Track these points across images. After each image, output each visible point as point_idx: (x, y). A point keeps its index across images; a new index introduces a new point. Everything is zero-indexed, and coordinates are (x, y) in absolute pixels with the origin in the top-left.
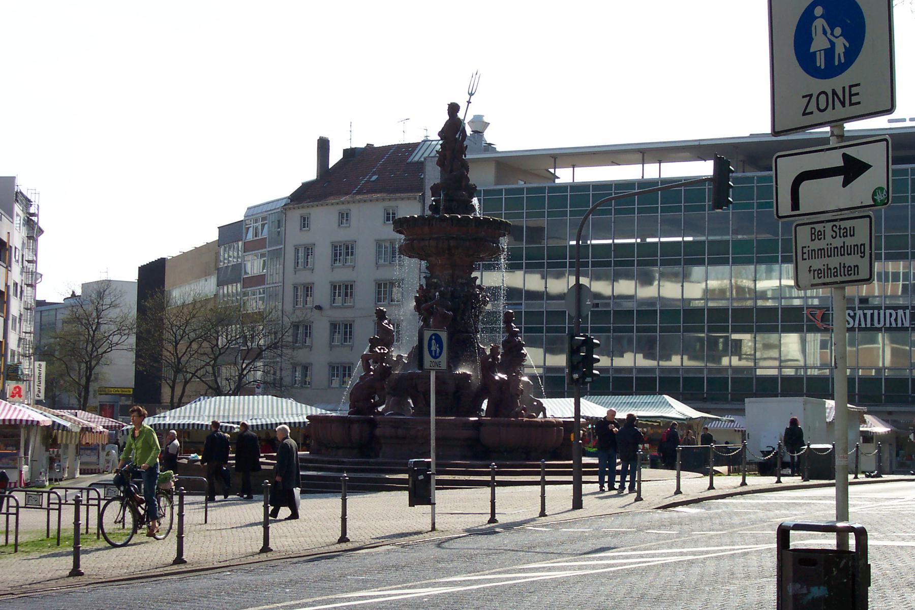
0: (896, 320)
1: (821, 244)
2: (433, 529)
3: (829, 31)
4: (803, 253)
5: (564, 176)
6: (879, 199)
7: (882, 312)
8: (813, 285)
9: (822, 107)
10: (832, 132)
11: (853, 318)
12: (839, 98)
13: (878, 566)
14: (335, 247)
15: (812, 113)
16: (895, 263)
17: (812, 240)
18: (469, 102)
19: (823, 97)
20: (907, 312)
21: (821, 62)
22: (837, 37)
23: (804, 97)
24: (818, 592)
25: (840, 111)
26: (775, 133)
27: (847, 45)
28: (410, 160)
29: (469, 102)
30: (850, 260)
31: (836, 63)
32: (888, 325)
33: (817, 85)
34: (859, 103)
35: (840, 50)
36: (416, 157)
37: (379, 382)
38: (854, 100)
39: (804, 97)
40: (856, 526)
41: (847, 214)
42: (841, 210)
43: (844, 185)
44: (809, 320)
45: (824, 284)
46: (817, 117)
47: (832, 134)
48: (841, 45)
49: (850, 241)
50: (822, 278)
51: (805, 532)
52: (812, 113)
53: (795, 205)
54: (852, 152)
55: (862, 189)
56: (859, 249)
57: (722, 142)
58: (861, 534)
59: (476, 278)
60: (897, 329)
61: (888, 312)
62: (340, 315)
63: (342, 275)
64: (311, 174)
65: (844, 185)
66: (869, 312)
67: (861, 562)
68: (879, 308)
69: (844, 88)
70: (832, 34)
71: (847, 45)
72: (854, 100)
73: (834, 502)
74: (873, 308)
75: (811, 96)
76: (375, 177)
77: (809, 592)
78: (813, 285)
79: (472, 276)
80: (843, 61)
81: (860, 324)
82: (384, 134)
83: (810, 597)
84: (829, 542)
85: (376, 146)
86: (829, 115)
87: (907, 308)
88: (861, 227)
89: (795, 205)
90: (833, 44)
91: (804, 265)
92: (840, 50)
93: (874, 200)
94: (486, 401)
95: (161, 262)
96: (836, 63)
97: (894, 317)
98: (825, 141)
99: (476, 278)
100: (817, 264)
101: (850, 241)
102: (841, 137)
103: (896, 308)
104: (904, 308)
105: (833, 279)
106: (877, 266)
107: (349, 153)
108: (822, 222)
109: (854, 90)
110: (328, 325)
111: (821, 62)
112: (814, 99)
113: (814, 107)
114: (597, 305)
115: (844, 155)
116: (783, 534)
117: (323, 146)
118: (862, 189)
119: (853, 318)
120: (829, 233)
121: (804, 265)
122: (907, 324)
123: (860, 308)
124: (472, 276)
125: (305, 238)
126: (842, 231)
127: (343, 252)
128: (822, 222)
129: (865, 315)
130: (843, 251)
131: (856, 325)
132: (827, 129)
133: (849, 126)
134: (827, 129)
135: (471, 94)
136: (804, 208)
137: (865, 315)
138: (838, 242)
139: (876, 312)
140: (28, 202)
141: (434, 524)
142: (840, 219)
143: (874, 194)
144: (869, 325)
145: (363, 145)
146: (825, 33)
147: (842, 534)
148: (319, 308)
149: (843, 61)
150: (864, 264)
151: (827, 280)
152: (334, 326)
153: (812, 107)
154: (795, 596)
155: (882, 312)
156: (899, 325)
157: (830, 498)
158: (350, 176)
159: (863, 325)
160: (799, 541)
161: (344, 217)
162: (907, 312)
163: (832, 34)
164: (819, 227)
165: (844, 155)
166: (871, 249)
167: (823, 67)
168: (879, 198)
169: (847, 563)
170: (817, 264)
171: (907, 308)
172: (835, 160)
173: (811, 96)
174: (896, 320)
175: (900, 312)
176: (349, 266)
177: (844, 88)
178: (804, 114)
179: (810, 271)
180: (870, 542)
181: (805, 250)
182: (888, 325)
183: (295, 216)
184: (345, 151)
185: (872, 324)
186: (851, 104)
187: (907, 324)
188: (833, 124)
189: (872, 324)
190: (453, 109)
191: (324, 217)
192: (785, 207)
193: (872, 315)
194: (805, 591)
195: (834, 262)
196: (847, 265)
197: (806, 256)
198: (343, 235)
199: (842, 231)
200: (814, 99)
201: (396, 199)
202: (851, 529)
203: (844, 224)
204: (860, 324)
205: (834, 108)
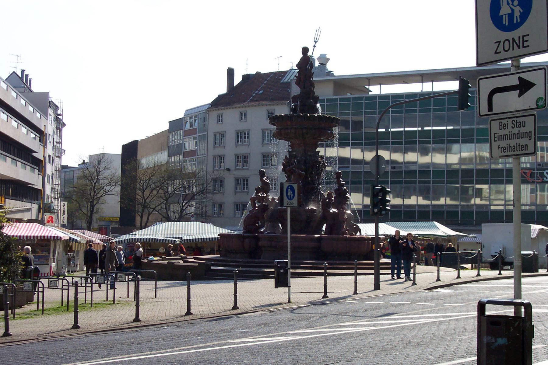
1: (506, 132)
2: (289, 301)
3: (510, 3)
4: (495, 137)
5: (374, 90)
6: (541, 104)
8: (501, 157)
9: (506, 49)
10: (512, 64)
12: (516, 43)
13: (539, 328)
15: (500, 52)
16: (542, 143)
17: (500, 129)
18: (314, 46)
19: (507, 43)
21: (506, 21)
22: (515, 6)
23: (495, 43)
24: (501, 341)
25: (517, 52)
26: (478, 65)
27: (522, 11)
28: (282, 81)
29: (314, 46)
30: (523, 142)
31: (515, 22)
33: (504, 35)
34: (528, 46)
35: (517, 14)
36: (286, 79)
37: (261, 215)
38: (526, 44)
39: (495, 43)
40: (524, 302)
41: (521, 114)
42: (517, 111)
43: (519, 96)
45: (507, 156)
46: (504, 55)
47: (513, 65)
48: (518, 11)
49: (522, 130)
50: (507, 152)
51: (493, 305)
52: (500, 52)
53: (490, 108)
54: (524, 76)
55: (529, 100)
56: (528, 135)
57: (353, 77)
58: (528, 307)
59: (319, 152)
63: (242, 150)
64: (224, 90)
65: (519, 96)
67: (528, 324)
69: (519, 37)
70: (512, 4)
71: (522, 11)
72: (526, 44)
73: (513, 286)
75: (500, 42)
76: (261, 92)
77: (496, 341)
78: (501, 157)
79: (317, 150)
80: (519, 21)
83: (496, 344)
84: (510, 311)
85: (262, 72)
86: (510, 53)
88: (529, 121)
89: (490, 108)
90: (513, 10)
91: (495, 145)
92: (517, 14)
93: (537, 105)
96: (515, 22)
98: (509, 69)
99: (319, 152)
100: (503, 144)
101: (522, 130)
102: (518, 67)
105: (513, 153)
106: (539, 144)
107: (246, 77)
108: (506, 118)
109: (525, 38)
111: (506, 21)
112: (502, 43)
113: (501, 49)
114: (394, 168)
115: (520, 79)
116: (481, 307)
117: (231, 73)
118: (529, 100)
120: (510, 125)
121: (495, 145)
124: (317, 150)
126: (518, 124)
127: (242, 136)
128: (506, 118)
130: (519, 136)
132: (510, 62)
133: (523, 61)
134: (510, 62)
135: (316, 42)
136: (495, 110)
138: (516, 131)
140: (56, 108)
141: (289, 299)
142: (517, 117)
143: (537, 101)
145: (254, 73)
146: (508, 4)
147: (517, 306)
148: (228, 170)
149: (519, 21)
150: (531, 144)
151: (509, 154)
152: (237, 180)
153: (501, 49)
154: (488, 345)
157: (511, 284)
158: (247, 91)
160: (491, 311)
161: (243, 115)
163: (512, 4)
164: (504, 121)
165: (520, 79)
166: (535, 135)
167: (507, 24)
168: (540, 103)
169: (519, 324)
170: (503, 144)
172: (514, 81)
173: (500, 42)
176: (246, 145)
177: (519, 37)
178: (496, 53)
179: (499, 148)
180: (533, 310)
181: (496, 135)
183: (214, 115)
184: (244, 76)
186: (524, 47)
188: (513, 59)
190: (305, 50)
191: (231, 115)
192: (484, 109)
194: (493, 340)
195: (513, 143)
196: (521, 145)
197: (496, 139)
198: (242, 126)
199: (518, 124)
200: (502, 43)
201: (274, 105)
202: (522, 304)
203: (519, 120)
205: (513, 50)
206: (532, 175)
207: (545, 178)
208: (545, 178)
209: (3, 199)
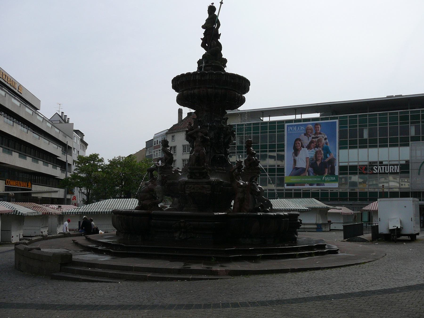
0: (394, 170)
5: (266, 119)
7: (388, 167)
11: (377, 169)
20: (398, 166)
32: (391, 172)
44: (359, 170)
60: (394, 173)
61: (391, 167)
64: (176, 122)
66: (383, 167)
68: (387, 165)
74: (385, 165)
81: (380, 171)
87: (398, 165)
97: (393, 168)
103: (394, 165)
104: (397, 165)
119: (377, 169)
122: (398, 171)
123: (379, 165)
129: (382, 168)
131: (378, 172)
137: (382, 168)
139: (386, 167)
140: (82, 135)
144: (383, 172)
155: (388, 167)
156: (395, 172)
159: (381, 172)
162: (398, 166)
171: (398, 165)
174: (394, 170)
175: (396, 167)
182: (391, 172)
185: (384, 171)
187: (398, 171)
189: (384, 171)
193: (384, 168)
204: (380, 171)
206: (366, 169)
207: (374, 171)
208: (374, 171)
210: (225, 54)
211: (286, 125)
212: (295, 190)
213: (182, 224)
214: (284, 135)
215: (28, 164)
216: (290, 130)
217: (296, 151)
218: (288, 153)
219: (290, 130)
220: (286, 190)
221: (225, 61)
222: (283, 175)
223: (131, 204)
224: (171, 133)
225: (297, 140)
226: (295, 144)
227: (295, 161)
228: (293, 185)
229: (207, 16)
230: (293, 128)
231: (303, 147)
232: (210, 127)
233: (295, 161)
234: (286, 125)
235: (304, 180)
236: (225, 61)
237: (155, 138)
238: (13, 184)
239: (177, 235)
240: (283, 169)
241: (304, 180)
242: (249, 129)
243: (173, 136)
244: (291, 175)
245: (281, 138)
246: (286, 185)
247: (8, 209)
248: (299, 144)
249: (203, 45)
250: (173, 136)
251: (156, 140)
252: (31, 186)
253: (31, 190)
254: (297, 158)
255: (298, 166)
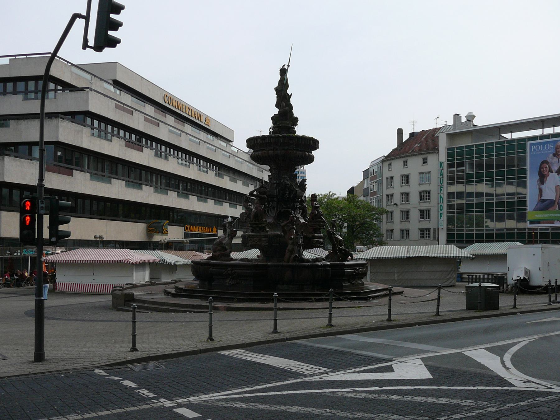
5: (508, 136)
14: (402, 176)
62: (405, 207)
63: (405, 189)
64: (395, 146)
82: (425, 125)
94: (308, 254)
95: (353, 188)
107: (412, 135)
110: (399, 212)
114: (520, 198)
117: (400, 132)
125: (389, 175)
127: (405, 179)
148: (396, 204)
152: (402, 212)
158: (415, 145)
161: (405, 162)
183: (386, 164)
184: (410, 134)
191: (397, 165)
198: (405, 172)
201: (427, 153)
209: (215, 229)
210: (296, 113)
211: (529, 143)
212: (541, 229)
213: (229, 272)
214: (525, 157)
215: (210, 207)
216: (534, 150)
217: (542, 178)
218: (532, 179)
219: (534, 150)
220: (530, 229)
221: (296, 120)
222: (526, 210)
223: (204, 256)
224: (387, 160)
225: (543, 163)
226: (540, 168)
227: (541, 191)
228: (538, 222)
229: (279, 77)
230: (538, 147)
231: (552, 172)
232: (277, 184)
233: (541, 191)
234: (529, 143)
235: (553, 215)
236: (296, 120)
237: (371, 166)
238: (194, 230)
239: (228, 281)
240: (525, 202)
241: (553, 215)
242: (479, 152)
243: (390, 165)
244: (535, 210)
245: (522, 160)
246: (528, 222)
247: (156, 258)
248: (546, 167)
249: (277, 106)
250: (390, 165)
251: (371, 170)
252: (217, 231)
253: (216, 236)
254: (543, 187)
255: (545, 197)
